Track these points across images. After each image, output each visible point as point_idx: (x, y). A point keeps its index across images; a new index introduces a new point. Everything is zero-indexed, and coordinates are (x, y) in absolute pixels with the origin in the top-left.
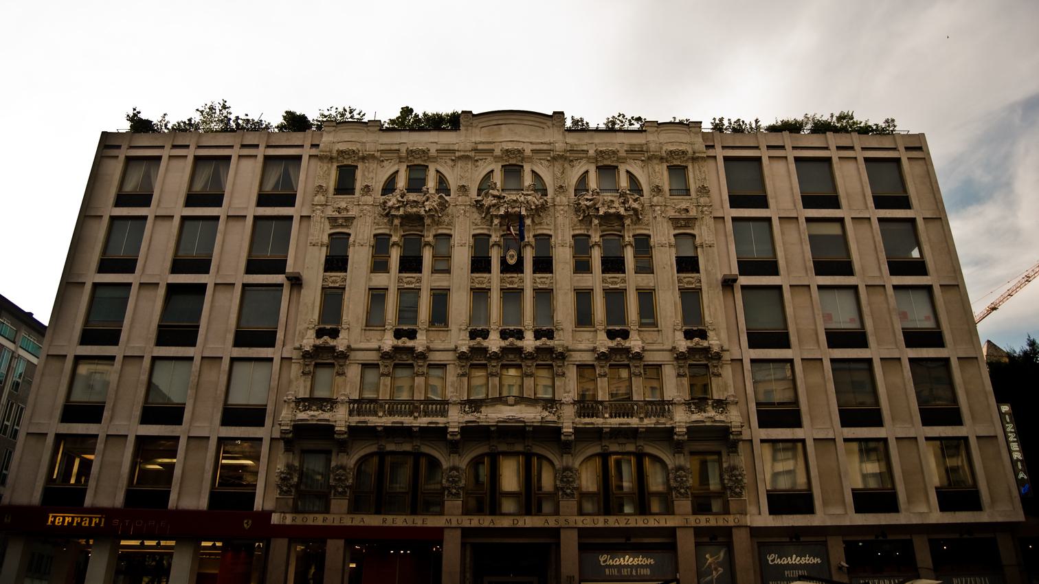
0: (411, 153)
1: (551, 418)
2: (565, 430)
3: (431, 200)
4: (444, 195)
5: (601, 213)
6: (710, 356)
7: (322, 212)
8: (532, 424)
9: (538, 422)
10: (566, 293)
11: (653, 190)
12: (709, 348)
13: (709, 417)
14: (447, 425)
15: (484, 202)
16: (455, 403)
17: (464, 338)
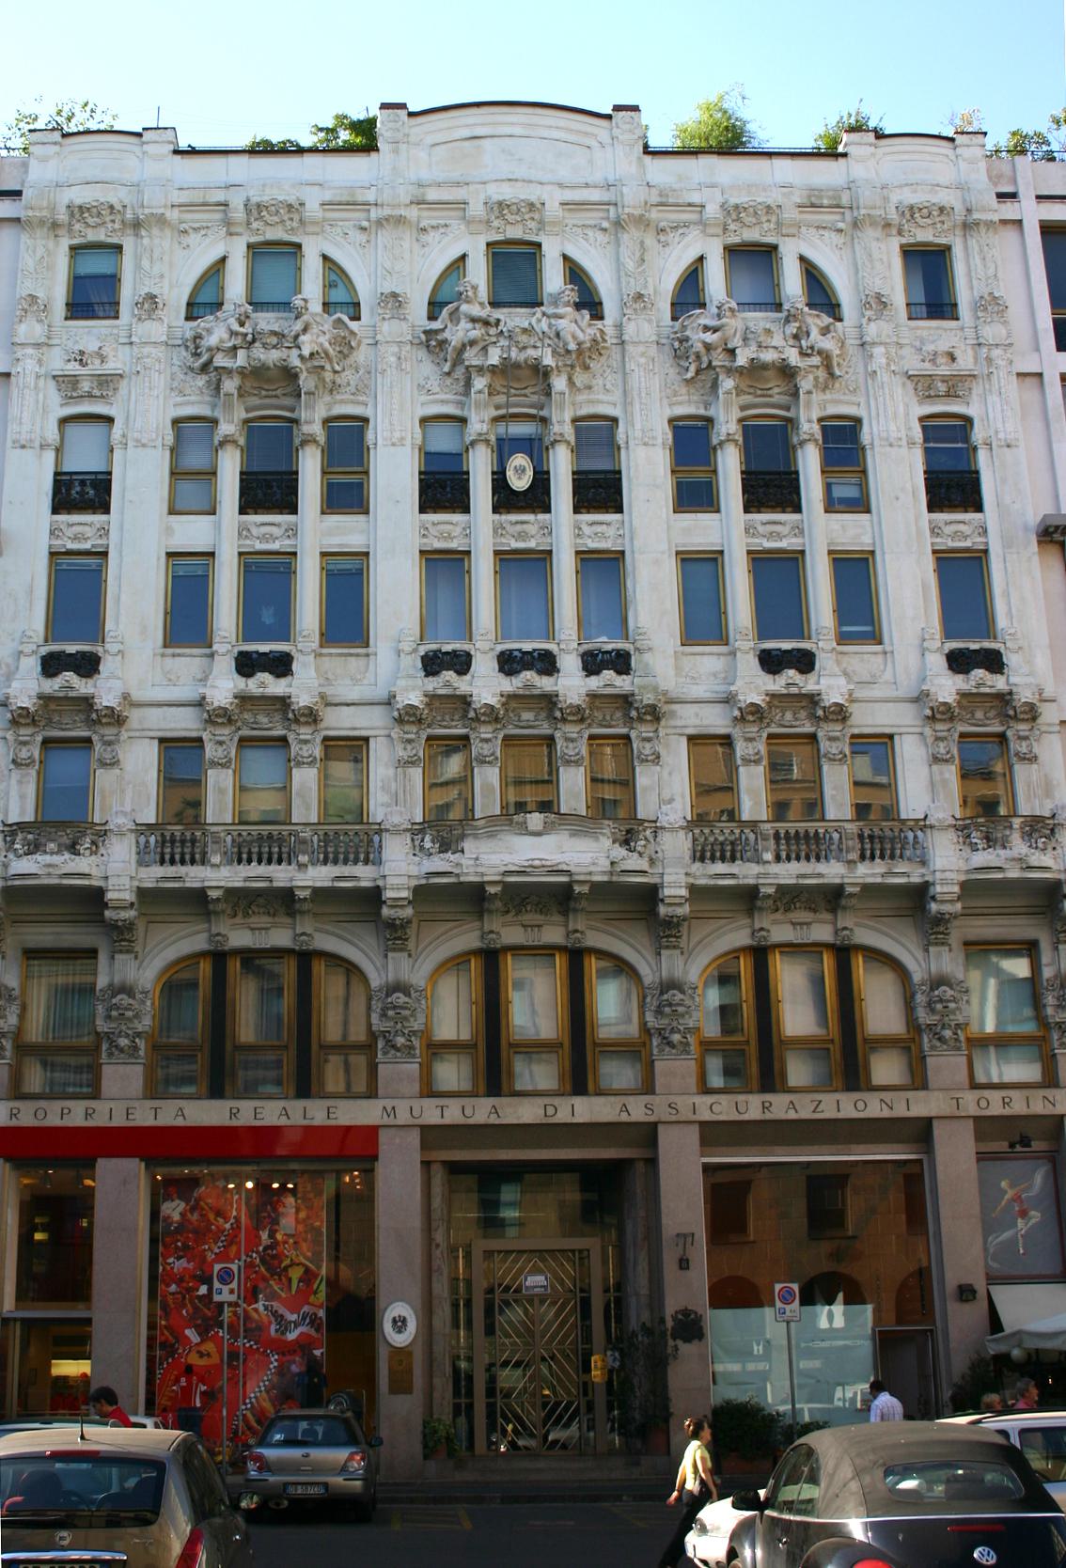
0: (256, 210)
1: (634, 862)
2: (667, 892)
3: (315, 331)
4: (345, 318)
5: (742, 360)
6: (1011, 713)
7: (40, 362)
8: (588, 878)
9: (604, 873)
10: (656, 562)
11: (867, 305)
12: (1011, 693)
13: (1014, 859)
14: (380, 883)
15: (447, 335)
16: (397, 832)
17: (411, 672)
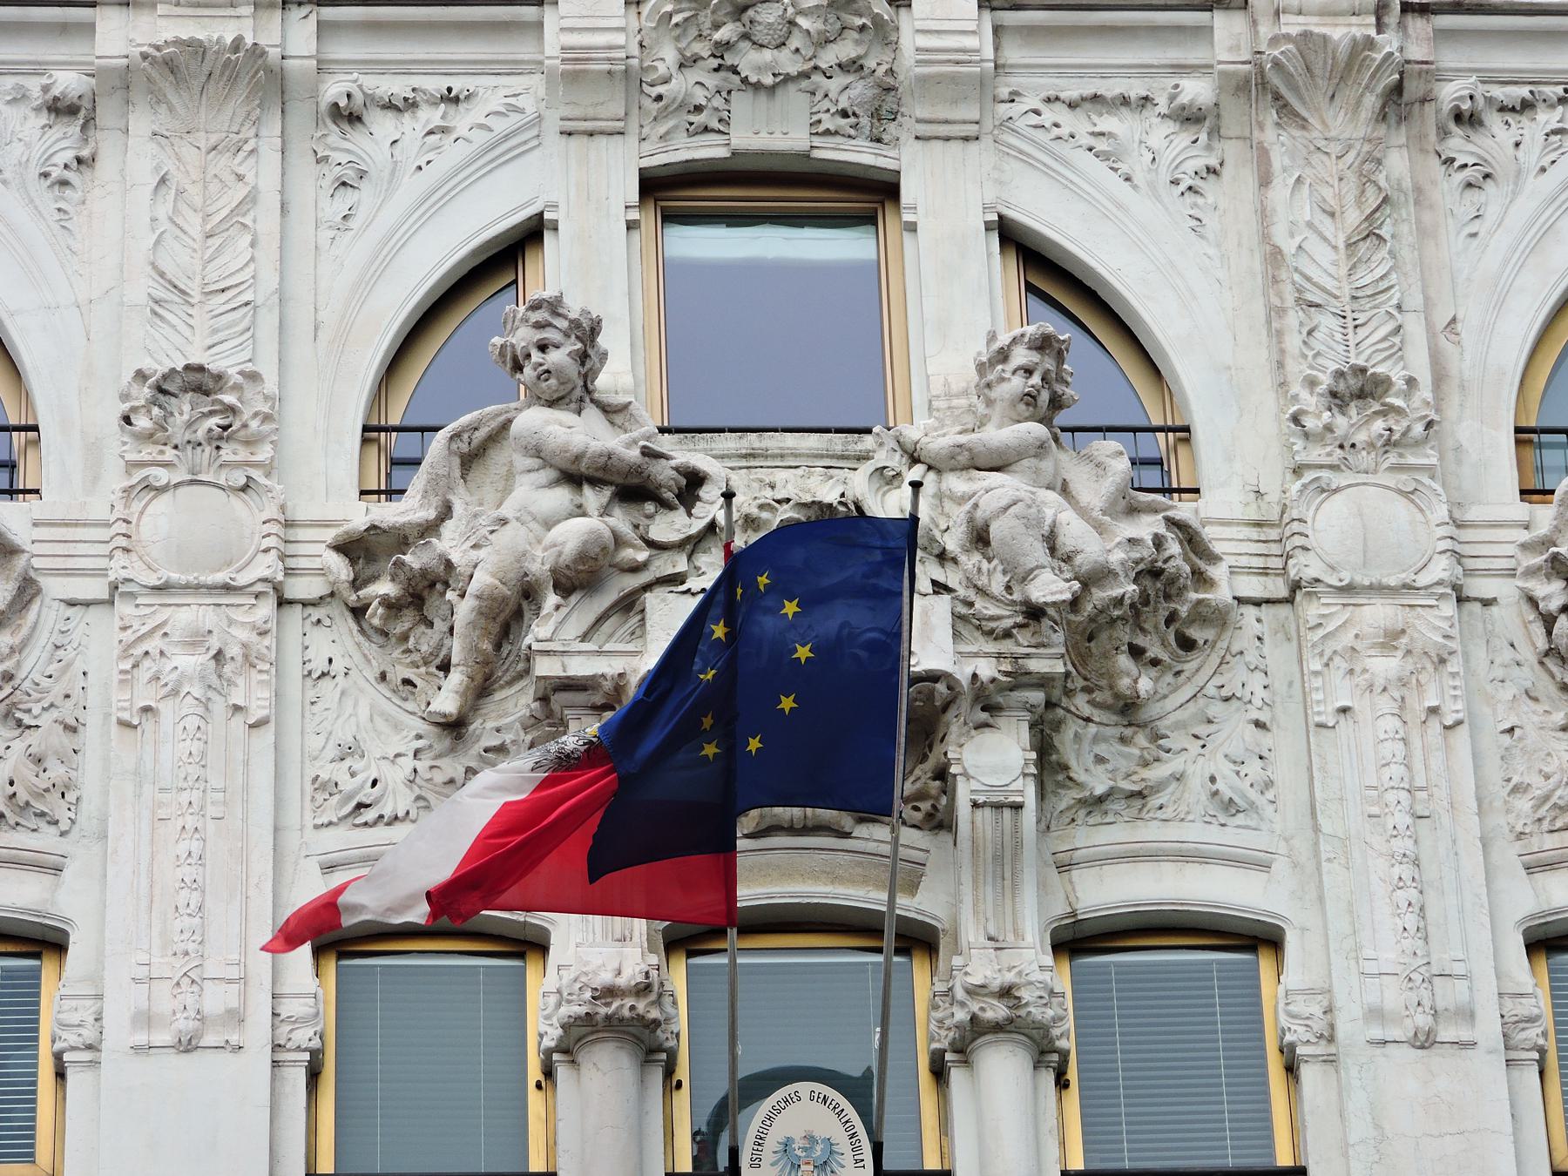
15: (451, 543)
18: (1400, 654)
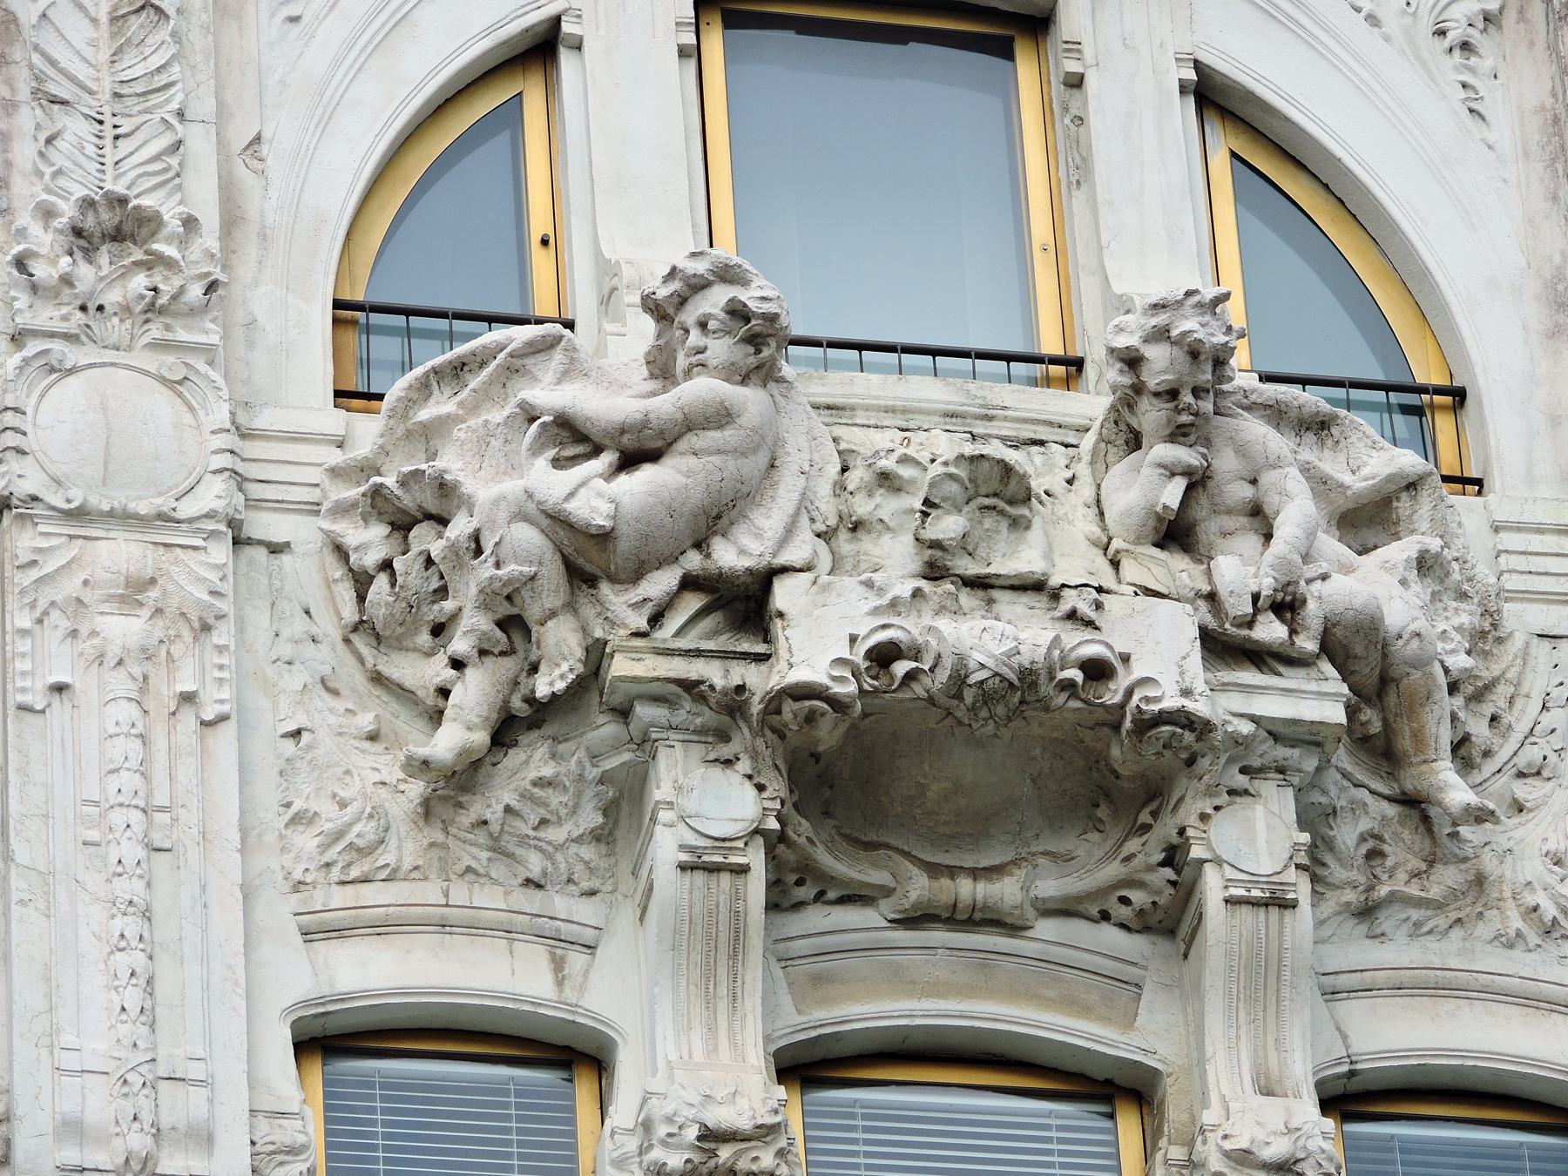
18: (146, 612)
